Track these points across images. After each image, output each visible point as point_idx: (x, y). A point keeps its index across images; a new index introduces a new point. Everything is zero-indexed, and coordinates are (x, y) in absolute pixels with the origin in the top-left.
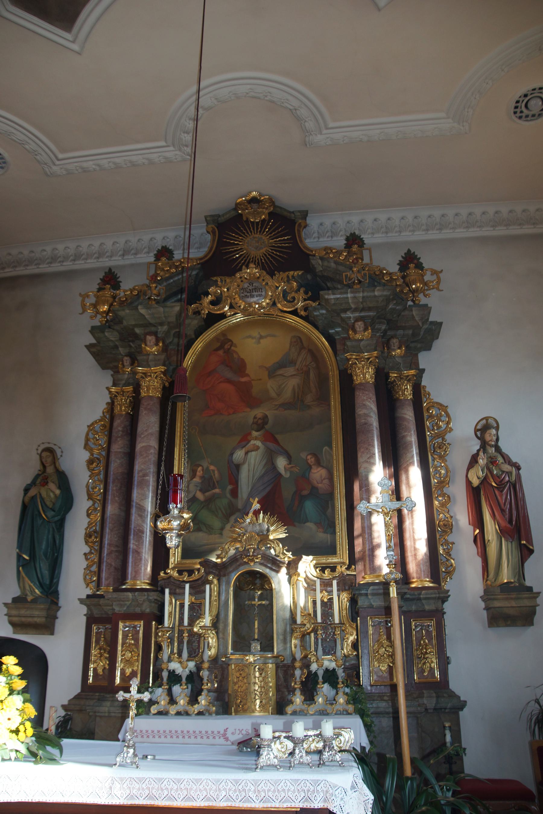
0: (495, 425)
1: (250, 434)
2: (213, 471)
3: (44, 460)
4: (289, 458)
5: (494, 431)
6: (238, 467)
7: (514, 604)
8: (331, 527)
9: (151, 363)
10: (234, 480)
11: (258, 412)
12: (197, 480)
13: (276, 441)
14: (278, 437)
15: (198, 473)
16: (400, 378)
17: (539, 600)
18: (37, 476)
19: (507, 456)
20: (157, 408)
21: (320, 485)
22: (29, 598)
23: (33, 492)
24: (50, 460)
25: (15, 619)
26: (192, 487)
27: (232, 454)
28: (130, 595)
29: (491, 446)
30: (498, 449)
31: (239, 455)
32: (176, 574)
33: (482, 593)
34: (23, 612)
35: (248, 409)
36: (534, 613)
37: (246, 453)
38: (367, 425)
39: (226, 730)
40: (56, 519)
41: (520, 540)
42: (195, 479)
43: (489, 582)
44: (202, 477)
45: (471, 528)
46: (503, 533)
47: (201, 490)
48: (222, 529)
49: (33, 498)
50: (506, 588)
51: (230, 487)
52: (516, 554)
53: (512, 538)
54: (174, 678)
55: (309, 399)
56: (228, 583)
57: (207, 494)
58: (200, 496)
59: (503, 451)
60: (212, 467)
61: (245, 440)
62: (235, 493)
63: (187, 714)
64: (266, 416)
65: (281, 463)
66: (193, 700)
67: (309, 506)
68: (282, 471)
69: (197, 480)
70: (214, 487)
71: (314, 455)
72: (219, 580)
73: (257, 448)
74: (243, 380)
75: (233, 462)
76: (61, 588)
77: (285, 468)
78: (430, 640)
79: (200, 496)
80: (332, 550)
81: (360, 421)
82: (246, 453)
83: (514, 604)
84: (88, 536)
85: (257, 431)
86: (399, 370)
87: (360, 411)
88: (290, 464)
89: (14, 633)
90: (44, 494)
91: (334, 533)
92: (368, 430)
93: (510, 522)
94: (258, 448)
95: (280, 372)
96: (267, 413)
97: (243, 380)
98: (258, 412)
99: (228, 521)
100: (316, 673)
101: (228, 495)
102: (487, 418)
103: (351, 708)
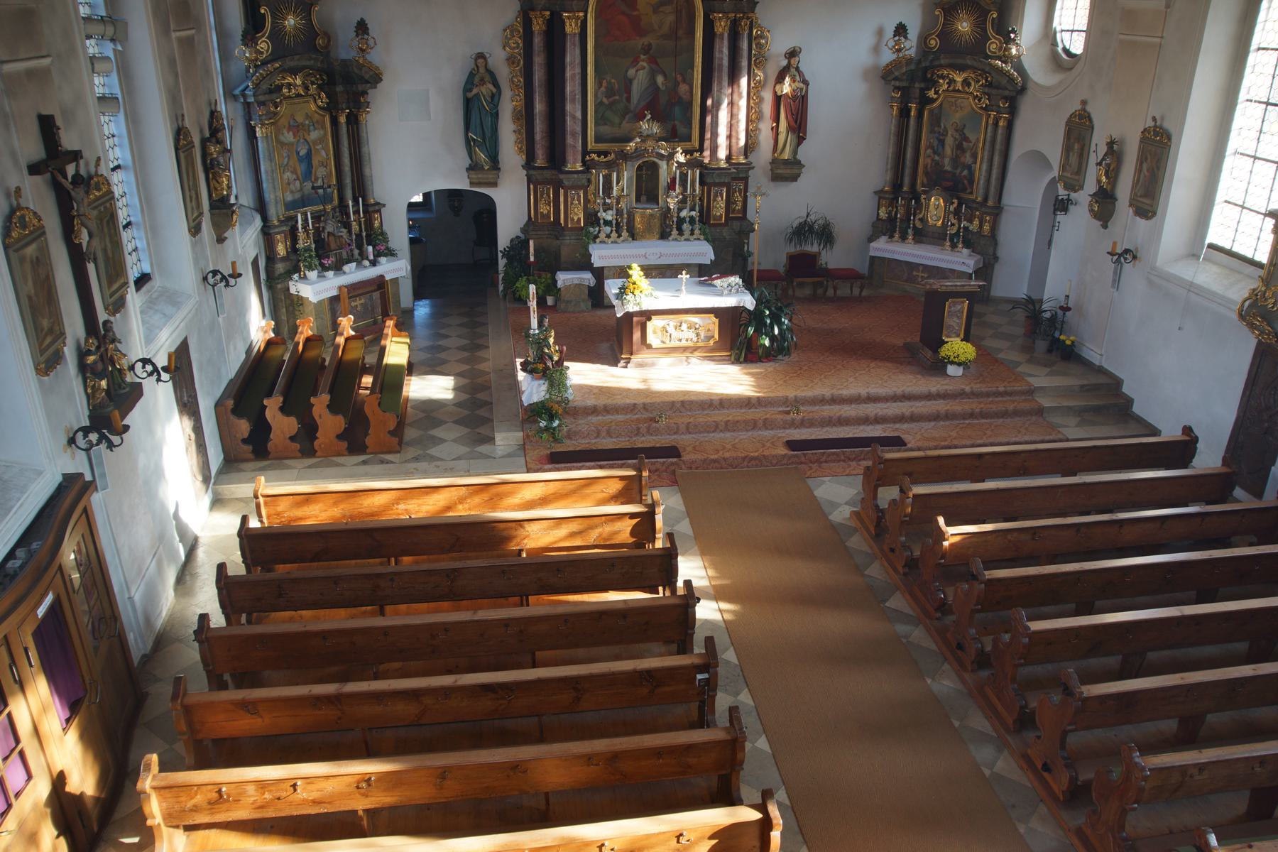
0: (799, 50)
1: (639, 57)
2: (614, 83)
3: (479, 65)
4: (665, 76)
5: (797, 59)
6: (631, 81)
7: (788, 171)
8: (689, 124)
9: (575, 9)
10: (628, 90)
11: (645, 40)
12: (603, 89)
13: (657, 63)
14: (659, 60)
15: (604, 85)
16: (743, 18)
17: (803, 170)
18: (471, 75)
19: (801, 72)
20: (577, 38)
21: (684, 97)
22: (486, 168)
23: (475, 91)
24: (484, 64)
25: (475, 181)
26: (599, 95)
27: (627, 71)
28: (576, 176)
29: (793, 67)
30: (797, 69)
31: (631, 72)
32: (596, 158)
33: (771, 161)
34: (480, 176)
35: (638, 38)
36: (799, 176)
37: (637, 71)
38: (721, 65)
39: (646, 253)
40: (494, 111)
41: (799, 133)
42: (602, 89)
43: (776, 155)
44: (606, 87)
45: (771, 122)
46: (790, 128)
47: (606, 97)
48: (620, 124)
49: (477, 95)
50: (786, 162)
51: (625, 95)
52: (795, 141)
53: (794, 133)
54: (607, 223)
55: (680, 33)
56: (633, 166)
57: (611, 99)
58: (605, 100)
59: (801, 69)
60: (613, 81)
61: (636, 61)
62: (629, 99)
63: (616, 242)
64: (650, 45)
65: (660, 79)
66: (619, 236)
67: (677, 110)
68: (661, 86)
69: (603, 89)
70: (615, 95)
71: (682, 75)
72: (626, 163)
73: (644, 68)
74: (635, 13)
75: (627, 77)
76: (500, 157)
77: (662, 84)
78: (740, 194)
79: (605, 100)
80: (689, 139)
81: (716, 62)
82: (637, 71)
83: (788, 171)
84: (516, 117)
85: (644, 55)
86: (744, 13)
87: (717, 54)
88: (665, 80)
89: (471, 187)
90: (485, 93)
91: (691, 128)
92: (720, 70)
93: (796, 122)
94: (644, 68)
95: (661, 9)
96: (651, 42)
97: (635, 13)
98: (645, 40)
99: (624, 118)
100: (684, 218)
101: (624, 100)
102: (794, 48)
103: (702, 237)
